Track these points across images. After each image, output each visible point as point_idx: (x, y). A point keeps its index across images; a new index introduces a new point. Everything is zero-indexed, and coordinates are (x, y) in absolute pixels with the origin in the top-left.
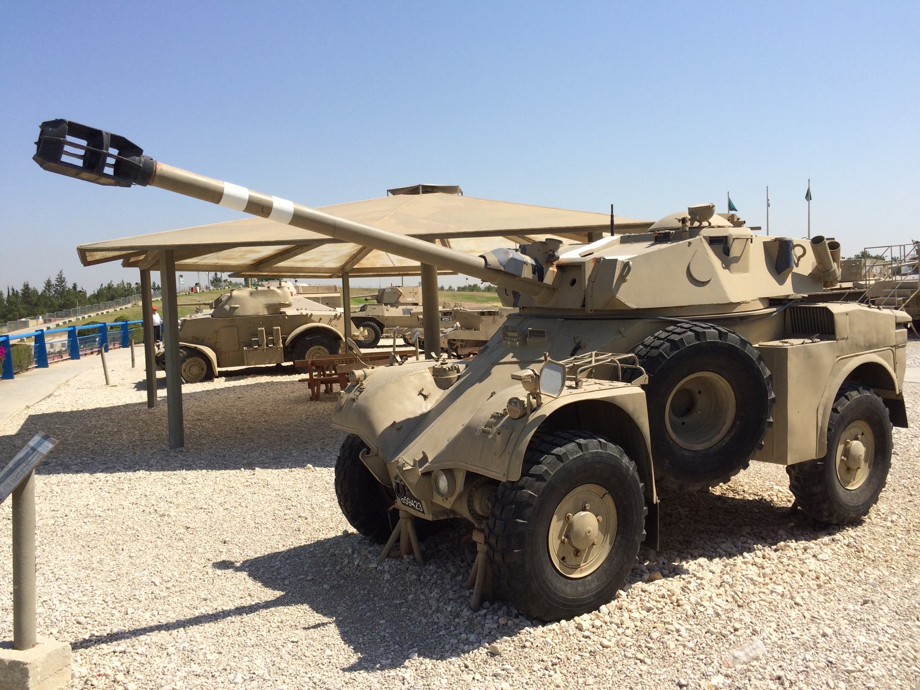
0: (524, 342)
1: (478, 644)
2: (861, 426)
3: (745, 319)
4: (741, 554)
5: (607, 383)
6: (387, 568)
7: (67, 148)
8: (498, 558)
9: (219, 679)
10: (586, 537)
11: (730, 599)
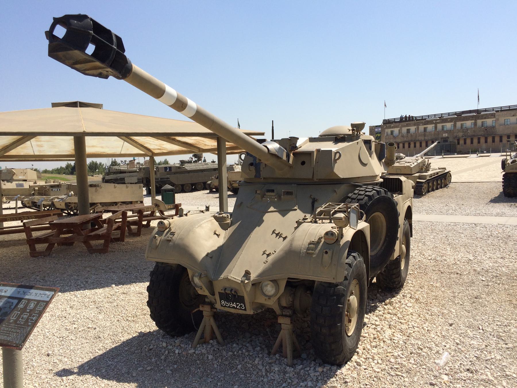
0: (279, 197)
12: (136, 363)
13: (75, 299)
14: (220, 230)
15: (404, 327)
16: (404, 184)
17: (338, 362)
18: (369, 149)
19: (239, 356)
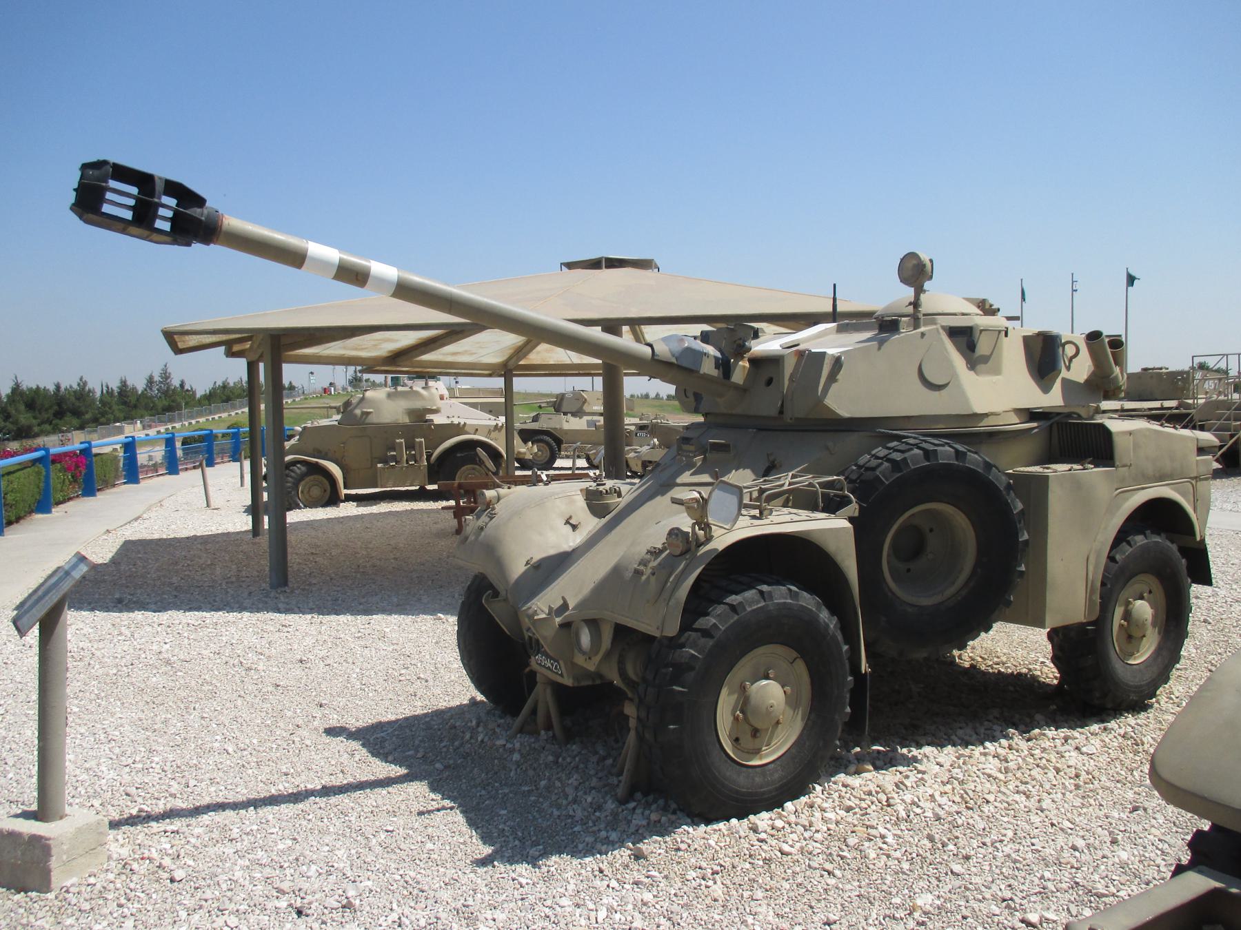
1: (621, 843)
2: (1146, 582)
3: (994, 436)
4: (982, 743)
5: (804, 514)
6: (517, 745)
7: (109, 196)
8: (648, 736)
9: (288, 872)
10: (768, 713)
11: (957, 799)
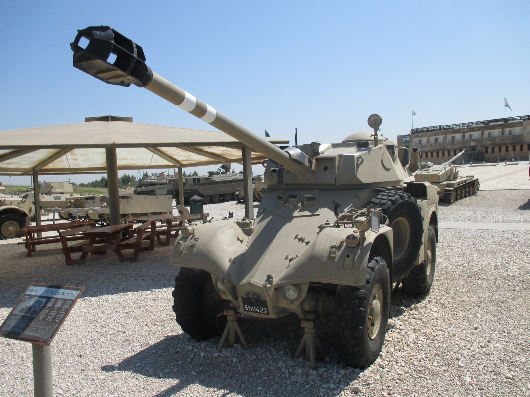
12: (163, 364)
13: (107, 304)
14: (243, 236)
15: (428, 331)
16: (428, 189)
17: (361, 364)
18: (392, 154)
19: (262, 359)
